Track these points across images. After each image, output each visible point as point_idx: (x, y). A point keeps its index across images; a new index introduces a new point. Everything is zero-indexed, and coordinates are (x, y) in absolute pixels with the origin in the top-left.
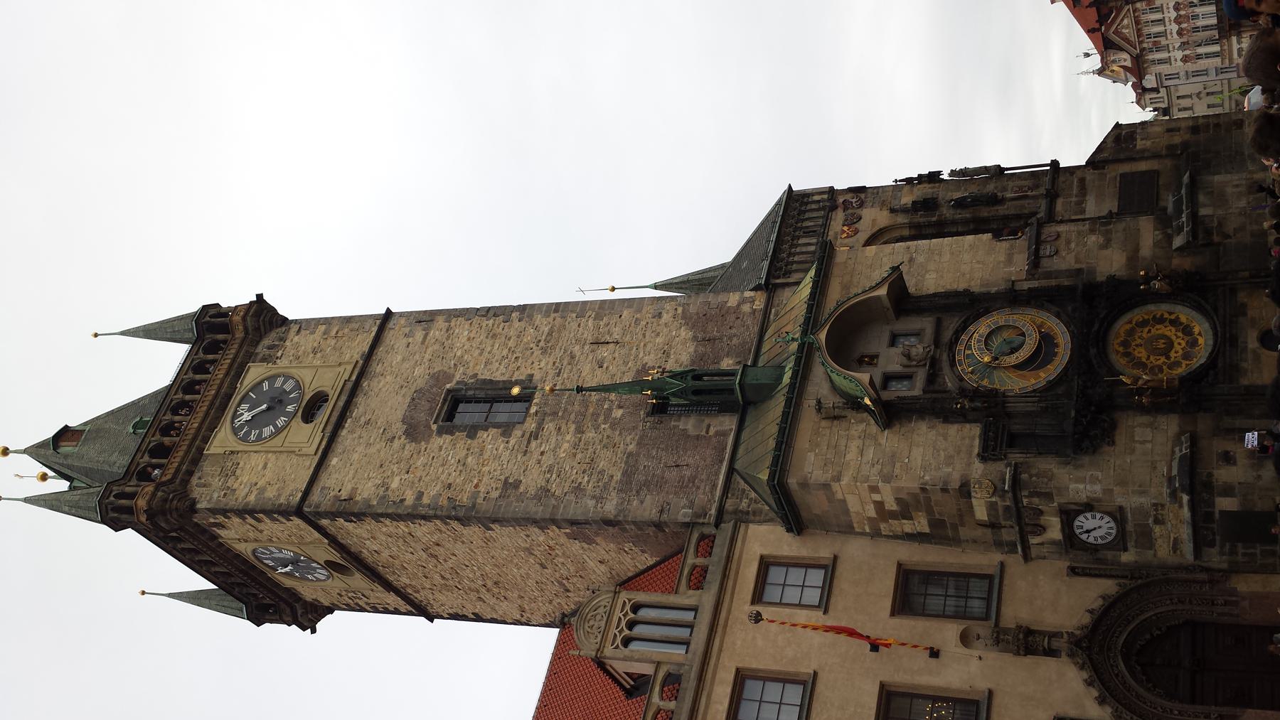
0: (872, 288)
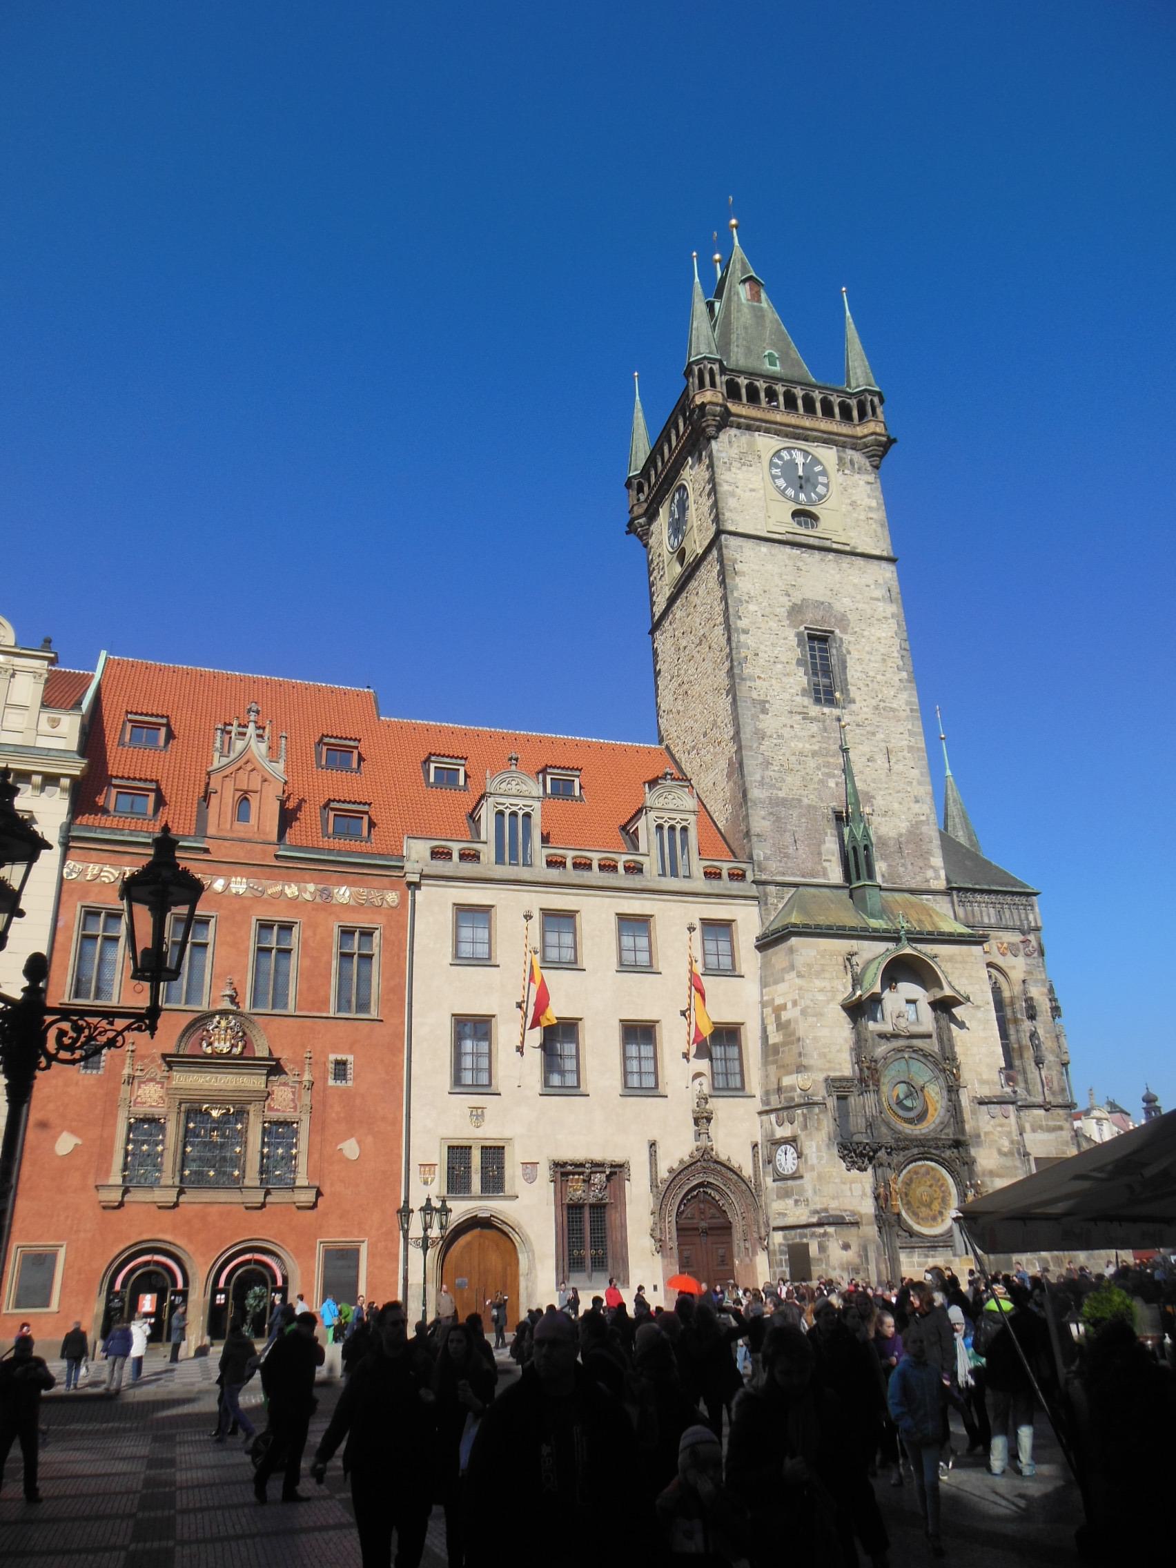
0: (950, 983)
